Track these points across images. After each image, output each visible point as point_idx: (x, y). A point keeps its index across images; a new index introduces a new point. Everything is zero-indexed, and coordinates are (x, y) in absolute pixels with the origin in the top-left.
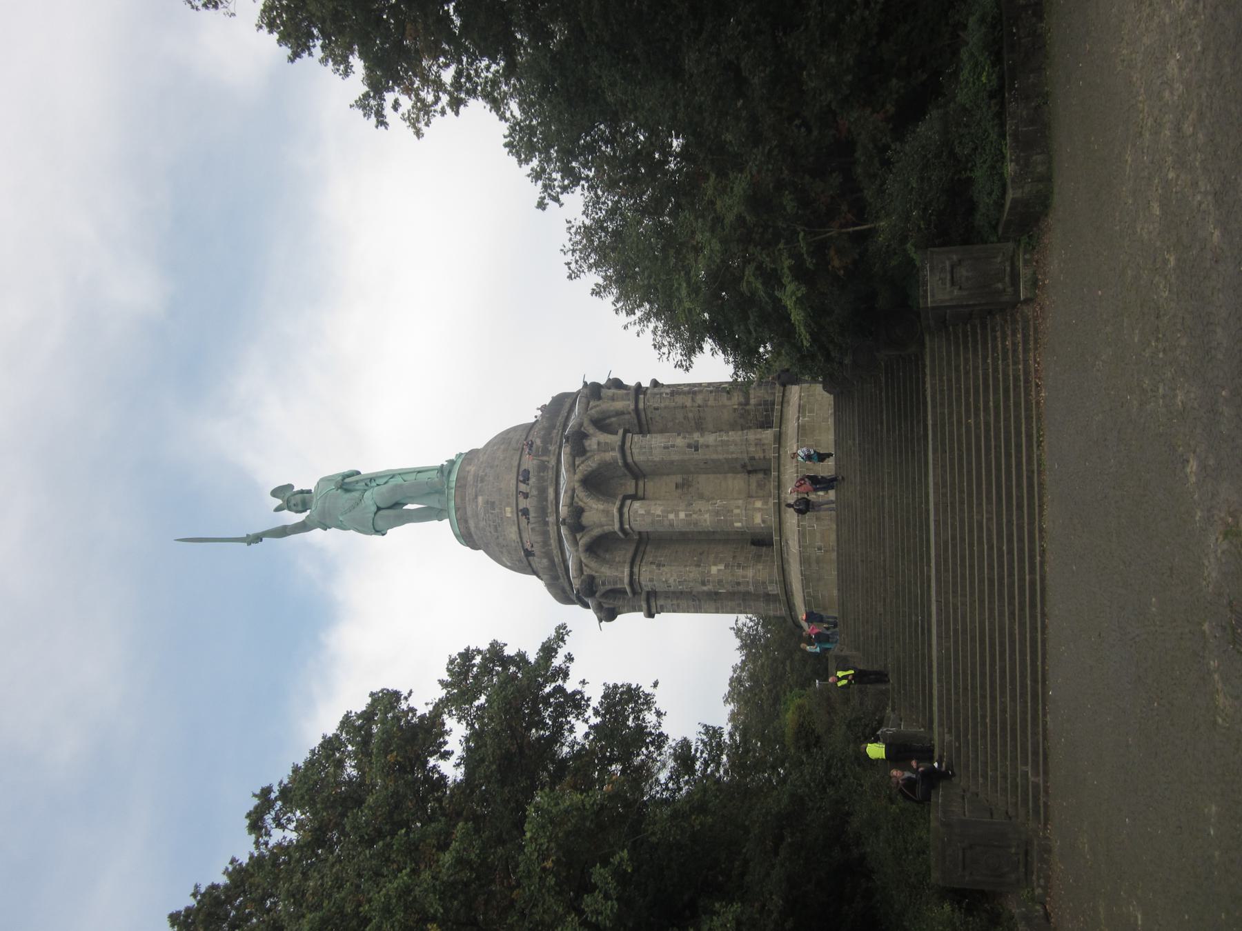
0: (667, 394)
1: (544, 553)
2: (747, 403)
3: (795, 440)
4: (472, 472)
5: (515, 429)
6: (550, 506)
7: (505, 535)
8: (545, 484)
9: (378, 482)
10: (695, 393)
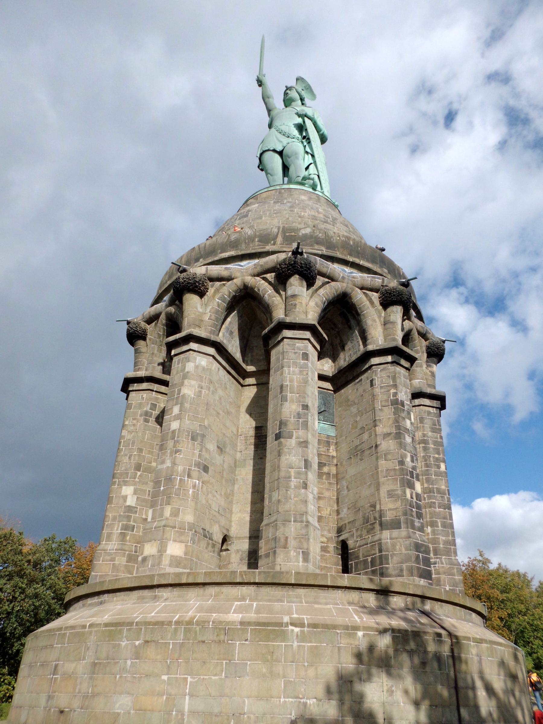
0: (395, 394)
2: (383, 526)
3: (252, 616)
8: (243, 246)
9: (307, 147)
10: (398, 436)
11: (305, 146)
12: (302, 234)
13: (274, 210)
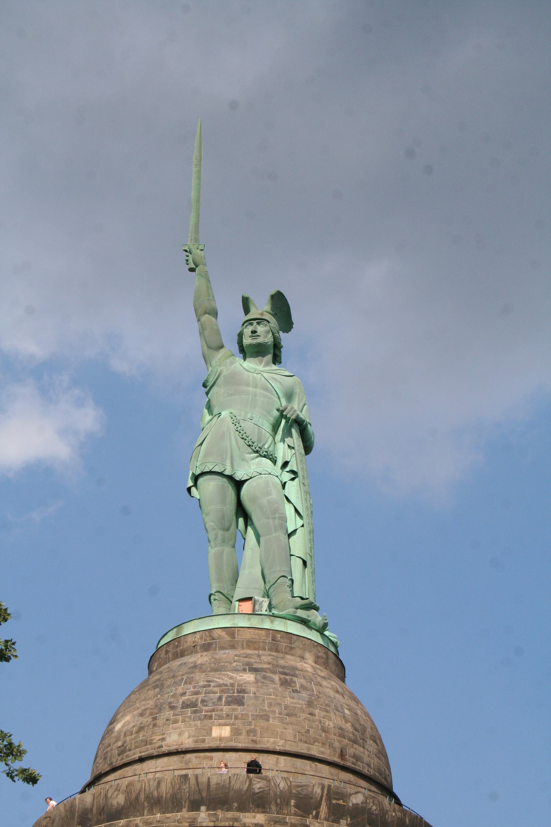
1: (137, 798)
4: (299, 664)
5: (382, 754)
6: (230, 814)
7: (176, 722)
8: (273, 807)
11: (285, 483)
12: (353, 804)
13: (286, 707)
